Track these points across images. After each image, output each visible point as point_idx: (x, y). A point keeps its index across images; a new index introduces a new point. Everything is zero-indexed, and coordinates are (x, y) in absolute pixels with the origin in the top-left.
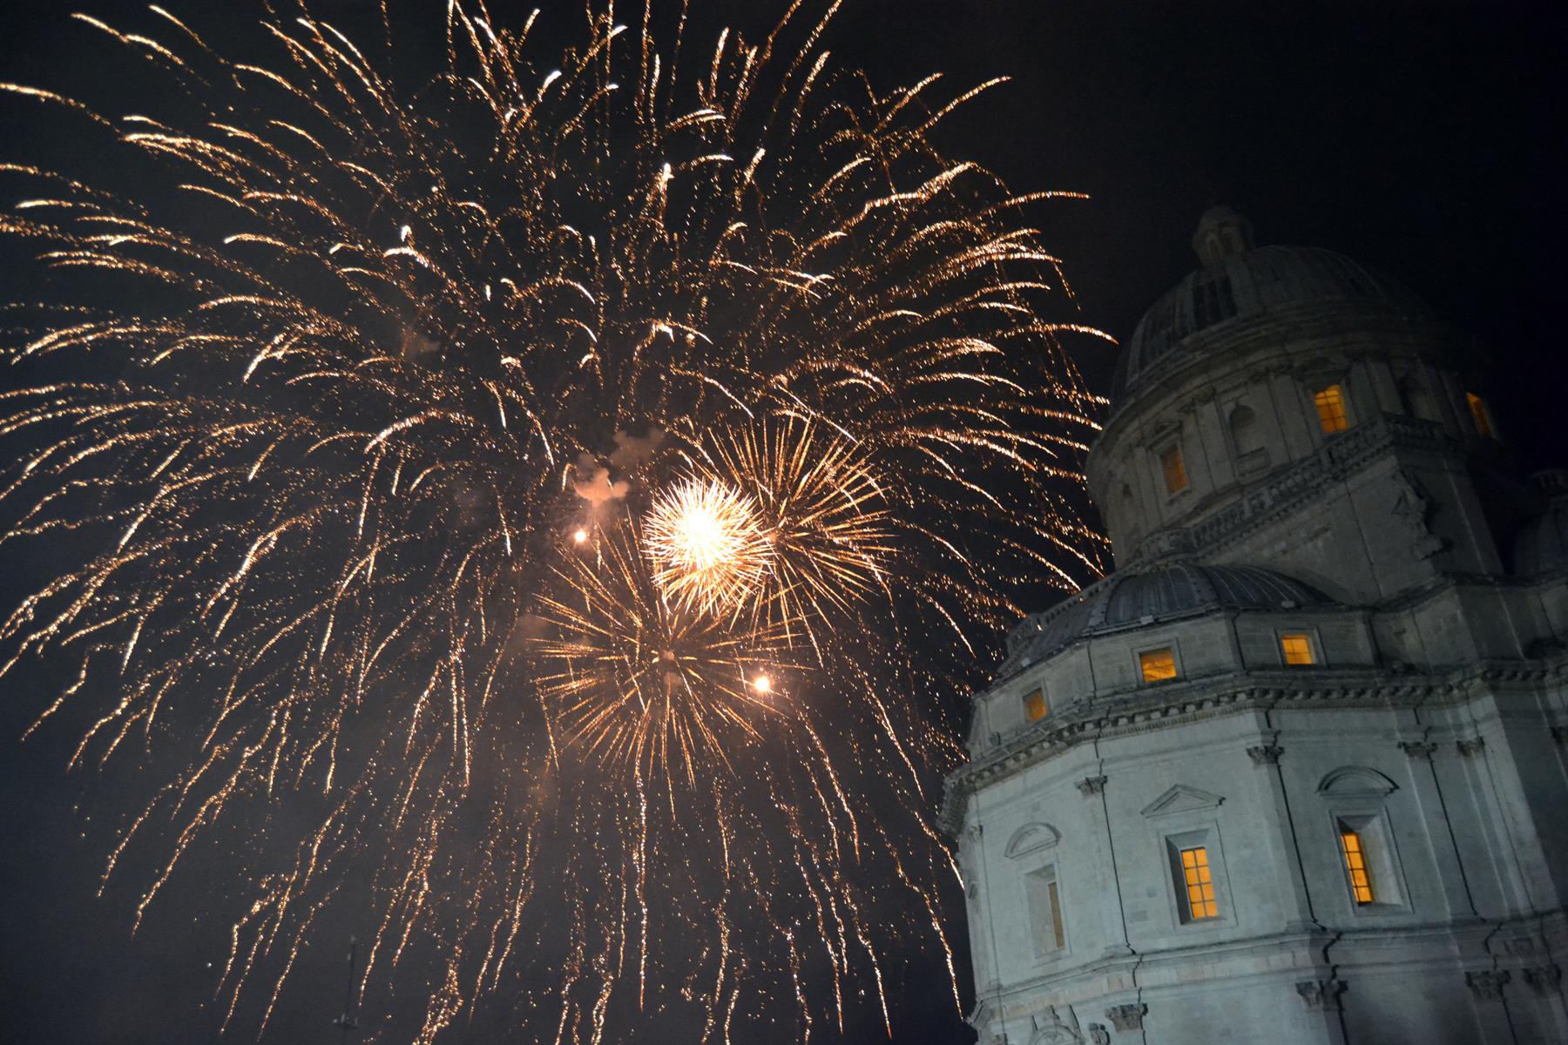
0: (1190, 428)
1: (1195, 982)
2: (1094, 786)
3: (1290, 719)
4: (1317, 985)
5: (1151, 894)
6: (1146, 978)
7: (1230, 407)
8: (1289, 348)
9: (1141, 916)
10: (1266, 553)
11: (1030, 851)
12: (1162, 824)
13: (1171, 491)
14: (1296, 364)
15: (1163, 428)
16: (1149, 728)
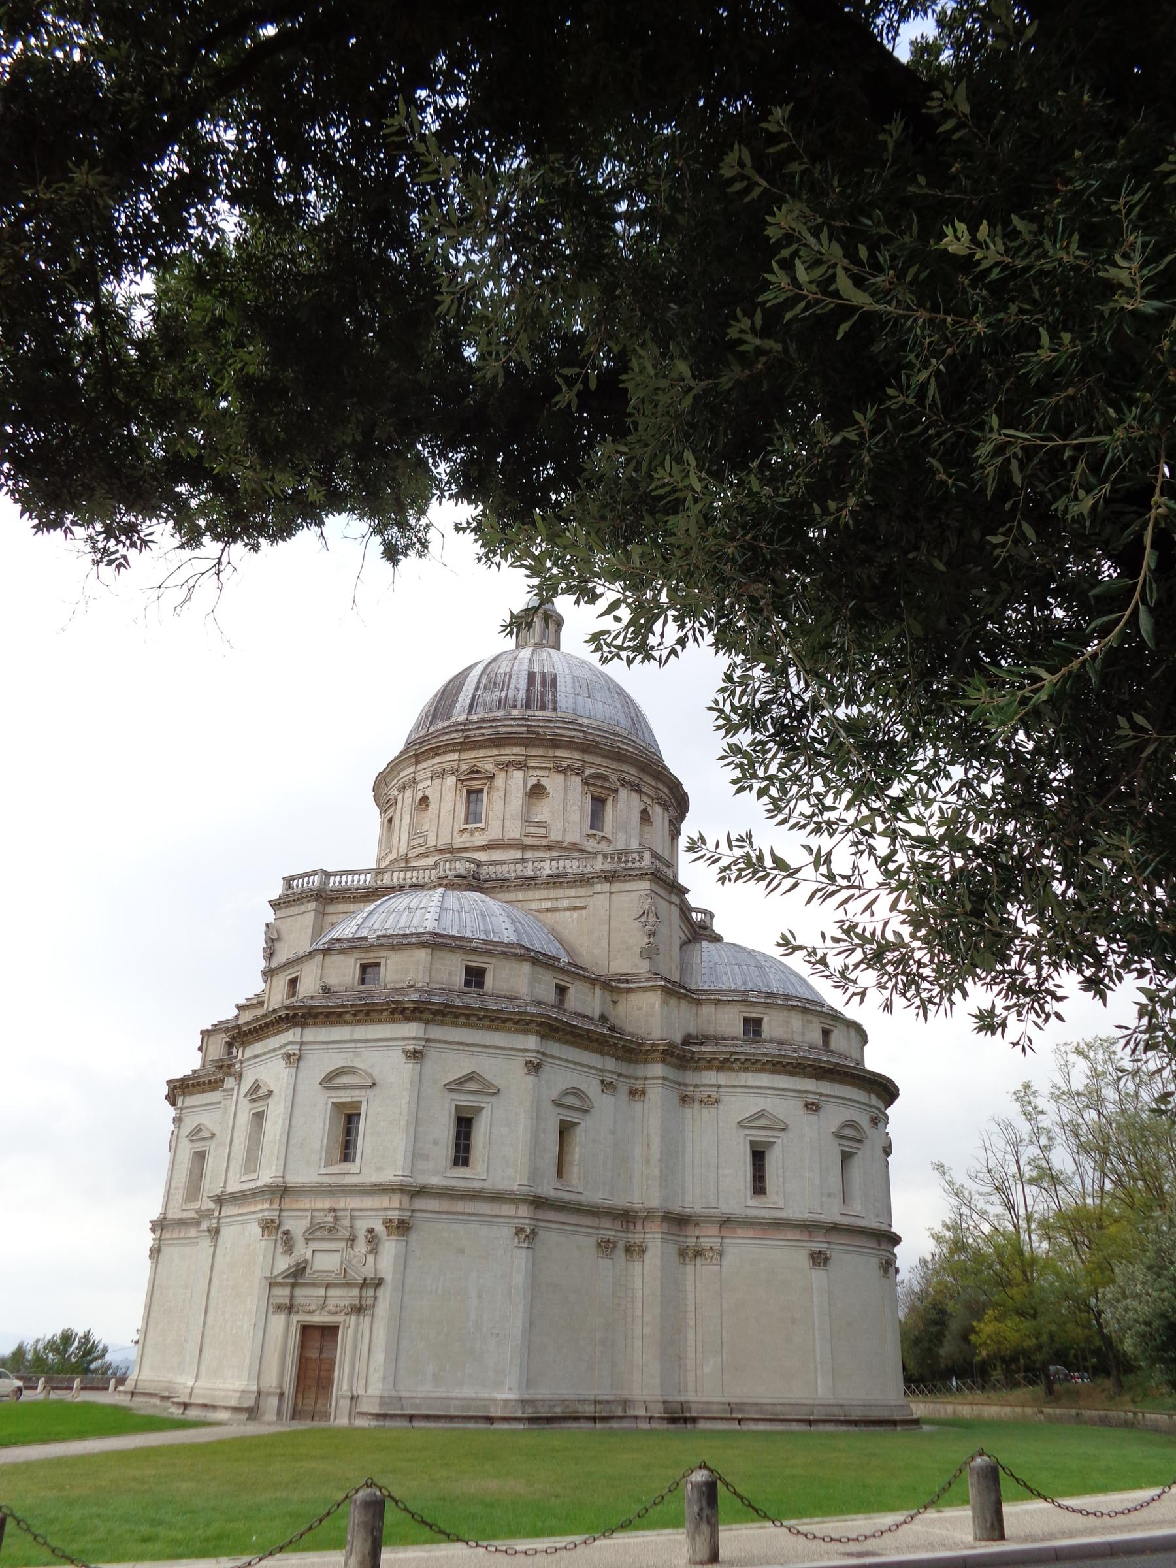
0: (499, 781)
1: (451, 1213)
2: (415, 1056)
3: (554, 1048)
4: (528, 1231)
5: (435, 1143)
6: (420, 1203)
7: (532, 781)
8: (587, 758)
9: (426, 1158)
10: (535, 905)
11: (344, 1087)
12: (455, 1096)
13: (467, 822)
14: (587, 772)
15: (478, 772)
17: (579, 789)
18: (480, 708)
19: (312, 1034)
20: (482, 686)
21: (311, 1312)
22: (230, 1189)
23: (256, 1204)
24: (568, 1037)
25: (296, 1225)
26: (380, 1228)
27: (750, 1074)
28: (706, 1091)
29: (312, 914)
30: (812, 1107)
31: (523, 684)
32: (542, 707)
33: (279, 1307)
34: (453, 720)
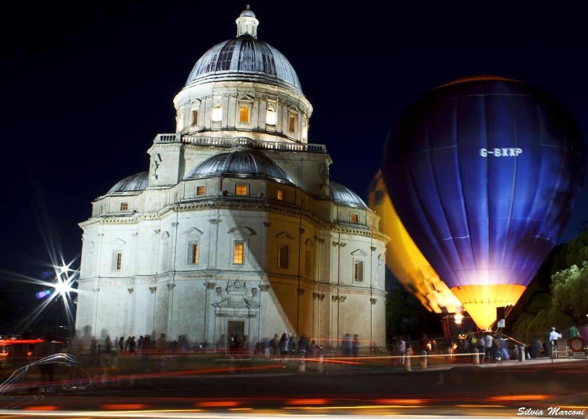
0: (256, 104)
15: (246, 99)
16: (283, 214)
17: (286, 112)
18: (243, 68)
19: (221, 211)
20: (242, 57)
21: (232, 317)
22: (176, 270)
23: (199, 276)
24: (310, 220)
25: (224, 286)
26: (259, 289)
27: (356, 236)
28: (341, 241)
29: (178, 153)
30: (373, 249)
31: (261, 60)
32: (270, 73)
33: (220, 315)
34: (230, 71)
